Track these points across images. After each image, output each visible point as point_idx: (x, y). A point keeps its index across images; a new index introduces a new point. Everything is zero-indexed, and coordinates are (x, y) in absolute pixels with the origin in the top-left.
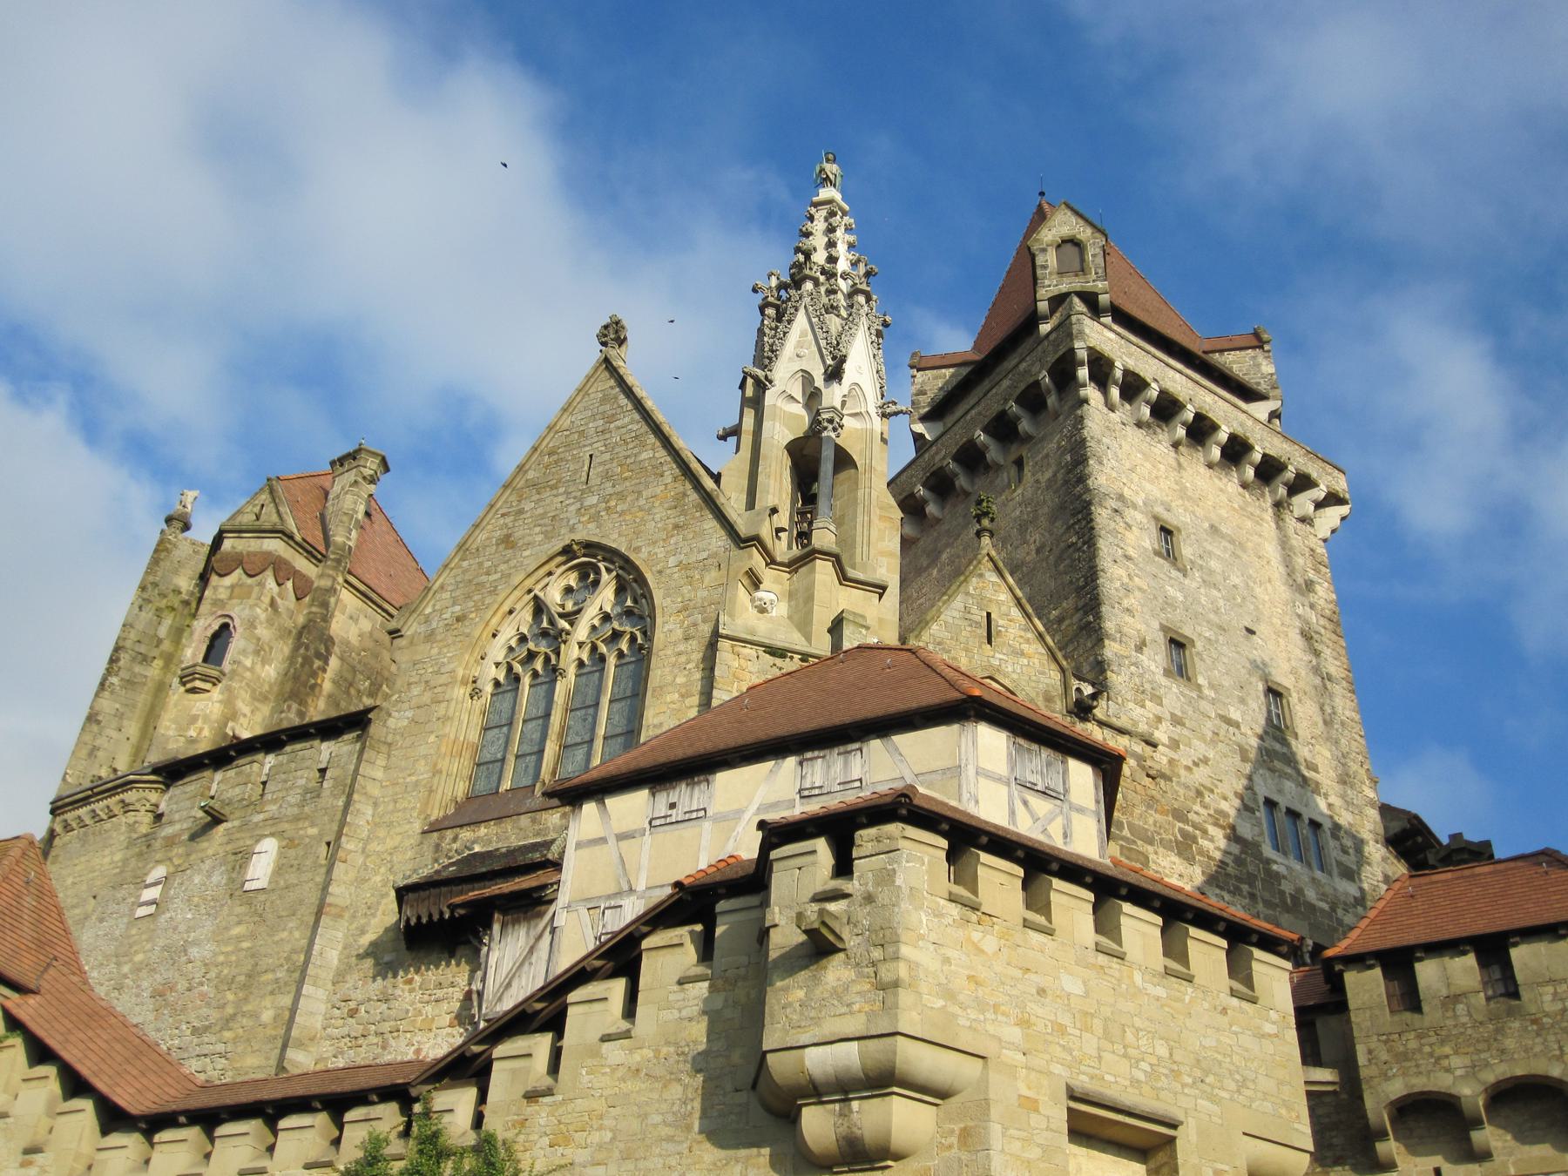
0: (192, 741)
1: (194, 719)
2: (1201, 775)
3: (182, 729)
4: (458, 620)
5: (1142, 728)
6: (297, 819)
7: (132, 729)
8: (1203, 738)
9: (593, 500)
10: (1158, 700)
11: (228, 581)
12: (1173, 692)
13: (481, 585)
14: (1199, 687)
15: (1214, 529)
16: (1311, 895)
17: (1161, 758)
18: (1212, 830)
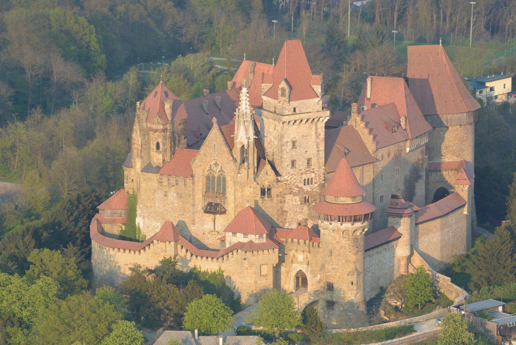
0: (160, 163)
1: (159, 159)
2: (294, 181)
3: (157, 161)
4: (201, 166)
5: (287, 179)
6: (184, 189)
7: (147, 156)
8: (296, 175)
9: (216, 153)
10: (289, 173)
11: (156, 134)
12: (292, 171)
13: (203, 161)
14: (296, 167)
15: (303, 136)
16: (309, 190)
17: (289, 182)
18: (295, 188)
